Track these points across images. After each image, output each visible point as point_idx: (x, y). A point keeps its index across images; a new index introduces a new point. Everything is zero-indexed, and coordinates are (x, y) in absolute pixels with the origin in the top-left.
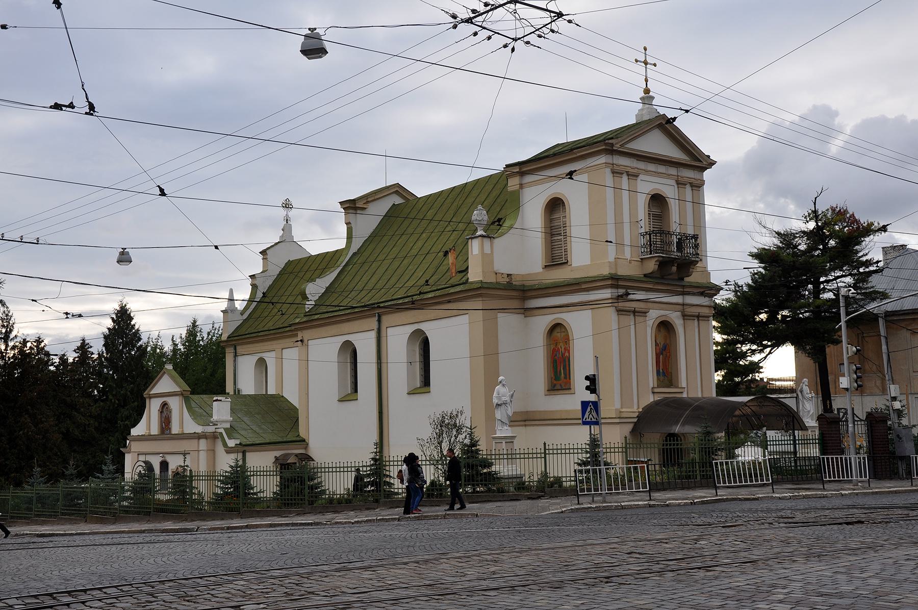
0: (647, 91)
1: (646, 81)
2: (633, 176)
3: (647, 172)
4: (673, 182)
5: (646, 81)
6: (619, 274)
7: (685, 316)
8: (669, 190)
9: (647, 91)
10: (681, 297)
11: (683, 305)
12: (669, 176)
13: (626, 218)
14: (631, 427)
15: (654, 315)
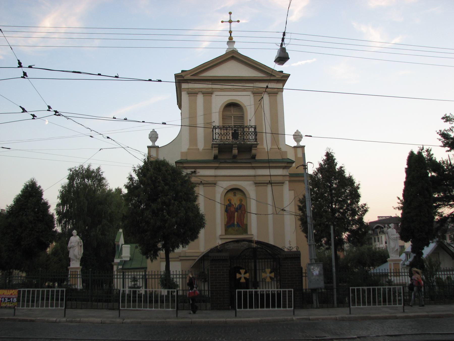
0: (231, 38)
1: (230, 32)
2: (208, 94)
3: (222, 90)
4: (249, 93)
5: (230, 32)
6: (188, 159)
7: (257, 184)
8: (246, 99)
9: (231, 38)
10: (268, 170)
11: (255, 176)
12: (244, 90)
13: (200, 121)
14: (192, 263)
15: (223, 185)
